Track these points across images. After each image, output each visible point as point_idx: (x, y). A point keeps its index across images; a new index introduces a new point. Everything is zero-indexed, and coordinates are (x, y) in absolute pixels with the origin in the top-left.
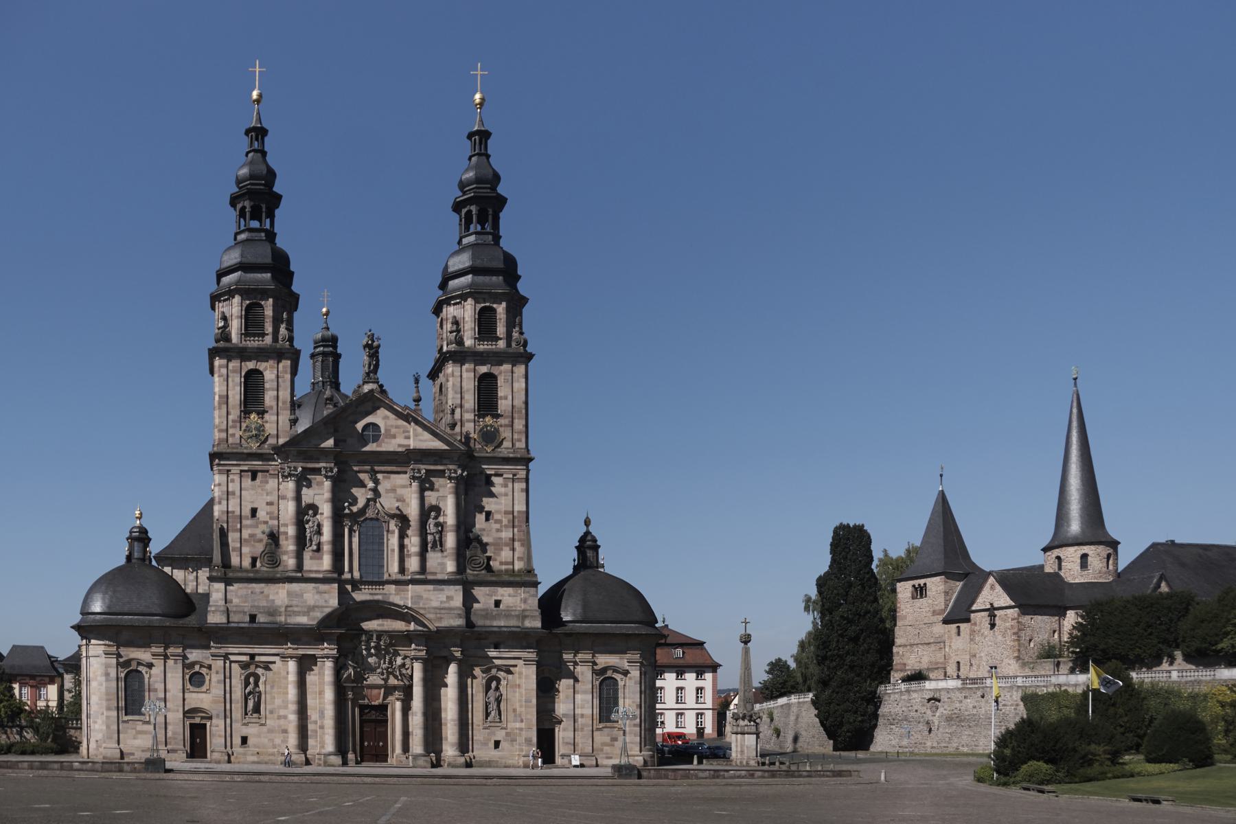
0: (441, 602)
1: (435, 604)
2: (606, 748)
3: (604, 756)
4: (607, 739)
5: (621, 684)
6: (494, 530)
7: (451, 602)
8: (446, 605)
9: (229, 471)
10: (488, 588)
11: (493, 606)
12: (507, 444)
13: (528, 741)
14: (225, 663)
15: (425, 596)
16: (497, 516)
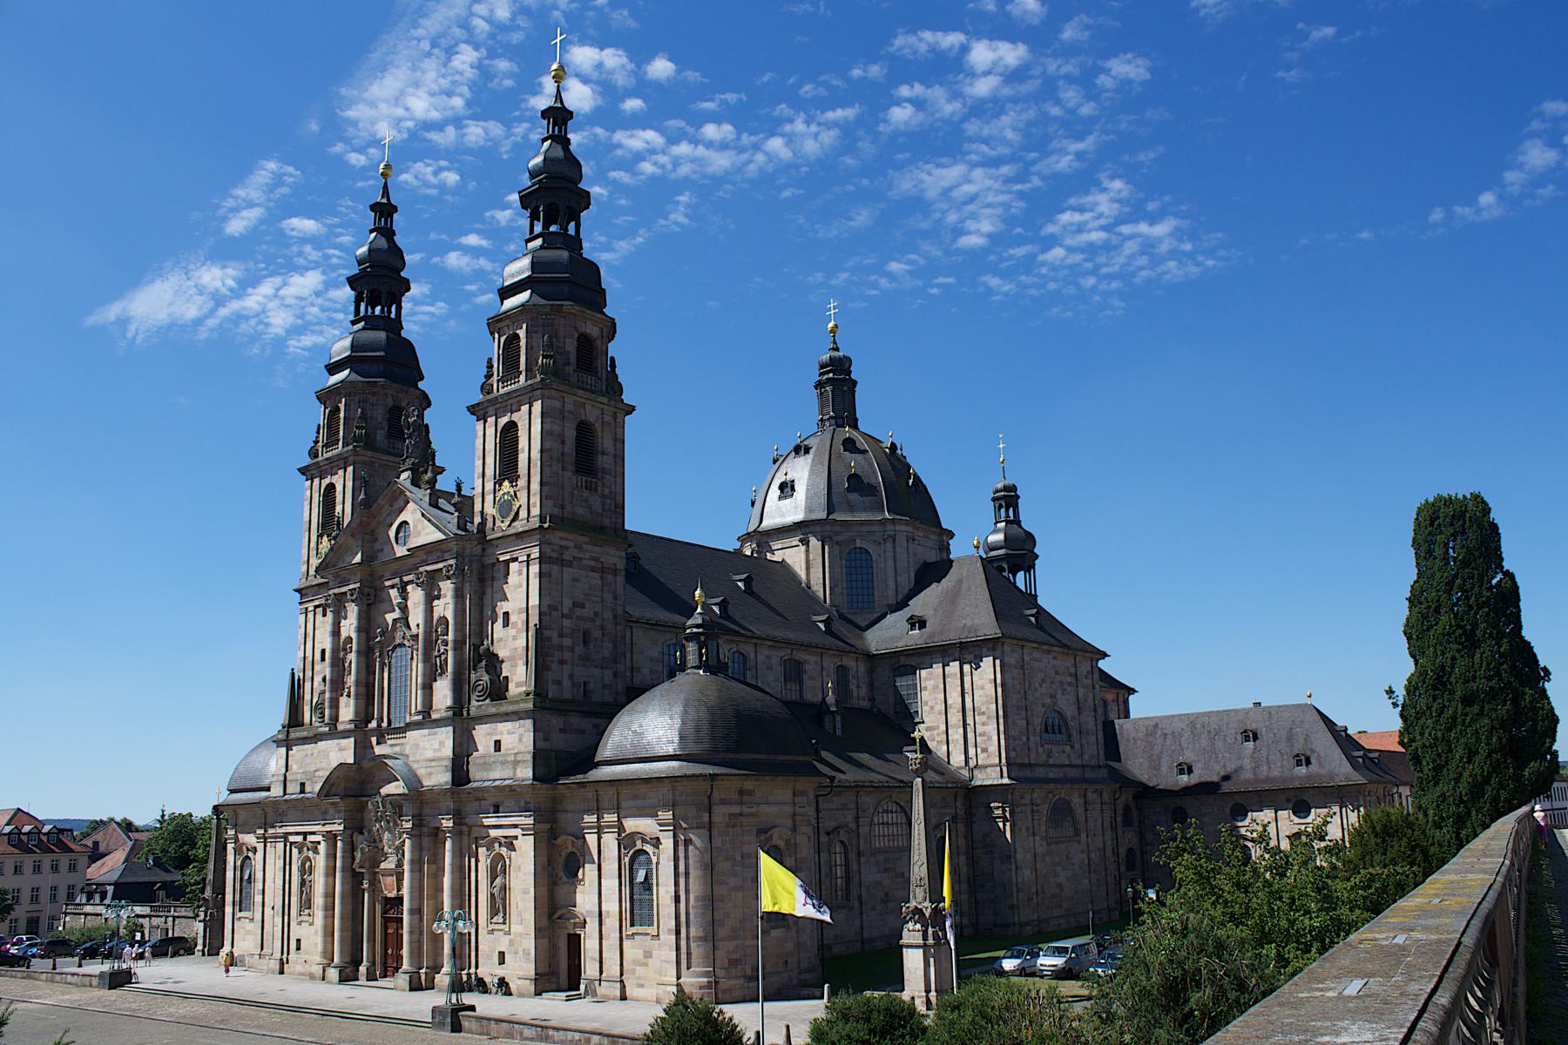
0: (435, 750)
1: (429, 754)
2: (640, 971)
3: (635, 981)
4: (640, 954)
5: (654, 860)
6: (510, 639)
7: (443, 749)
8: (438, 754)
9: (307, 609)
10: (488, 725)
11: (493, 750)
12: (523, 514)
13: (526, 953)
14: (285, 846)
15: (422, 744)
16: (513, 618)
